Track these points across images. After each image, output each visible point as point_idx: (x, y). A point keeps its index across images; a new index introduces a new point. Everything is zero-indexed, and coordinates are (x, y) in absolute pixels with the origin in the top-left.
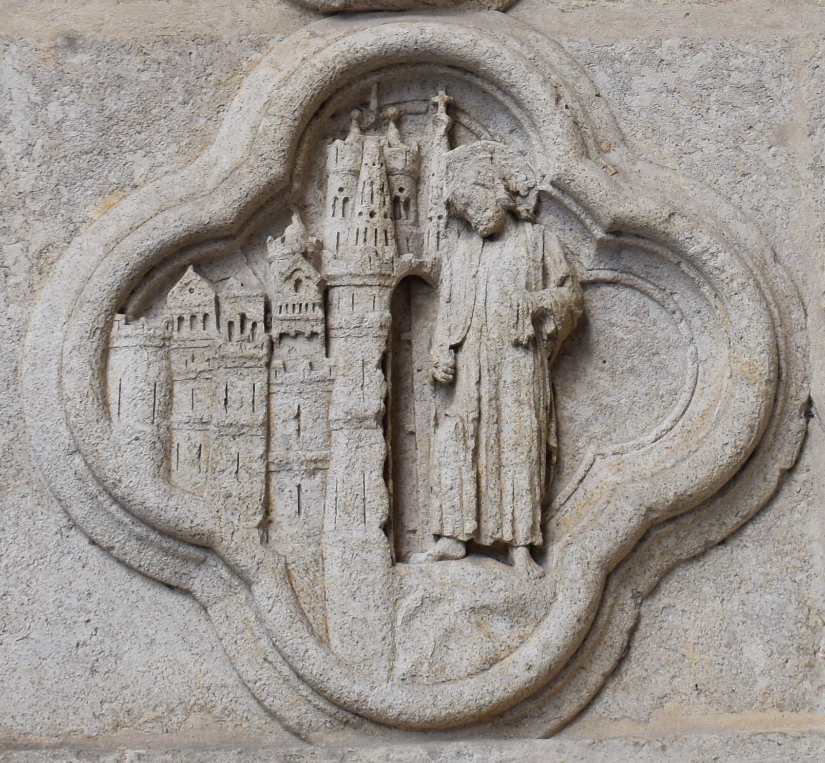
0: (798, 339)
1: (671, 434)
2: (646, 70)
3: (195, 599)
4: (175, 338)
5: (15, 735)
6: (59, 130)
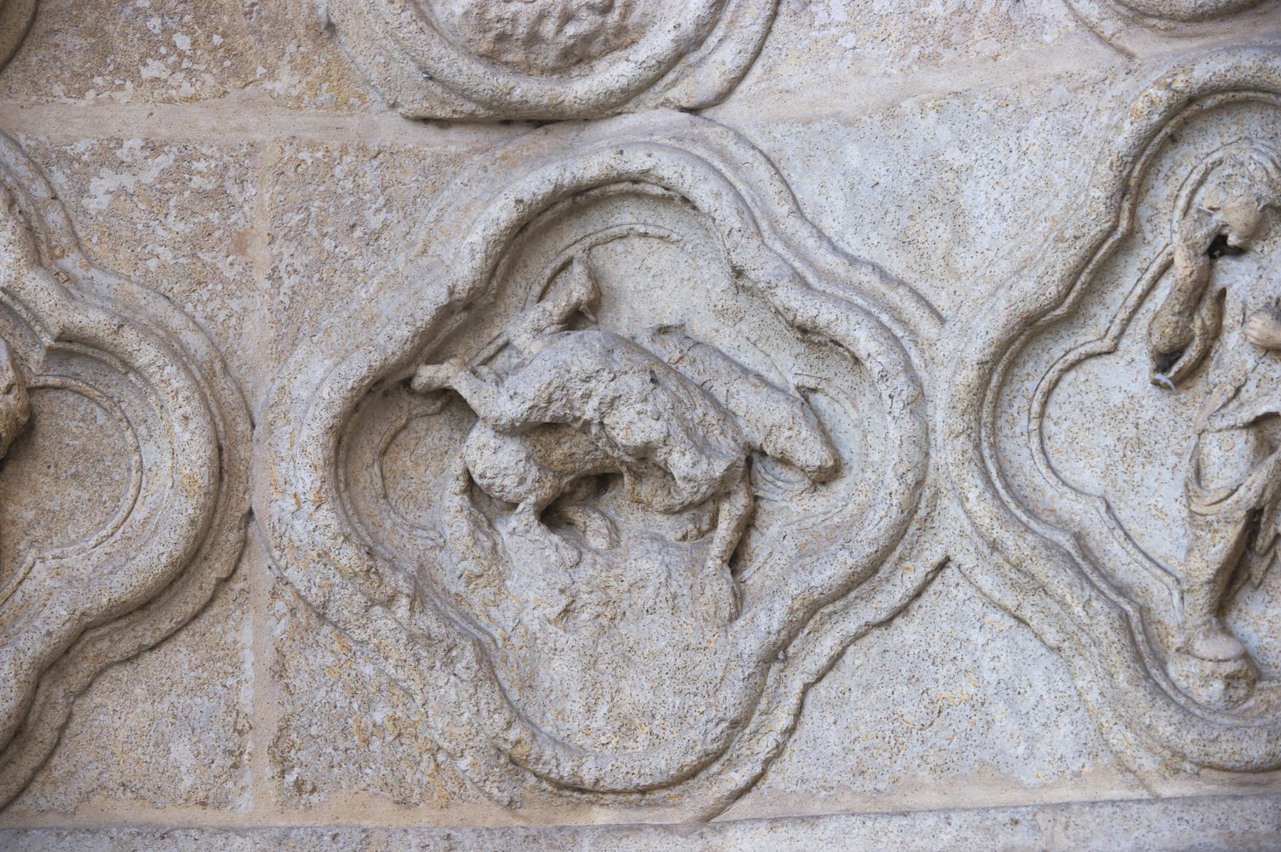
0: (242, 451)
1: (112, 540)
2: (105, 171)
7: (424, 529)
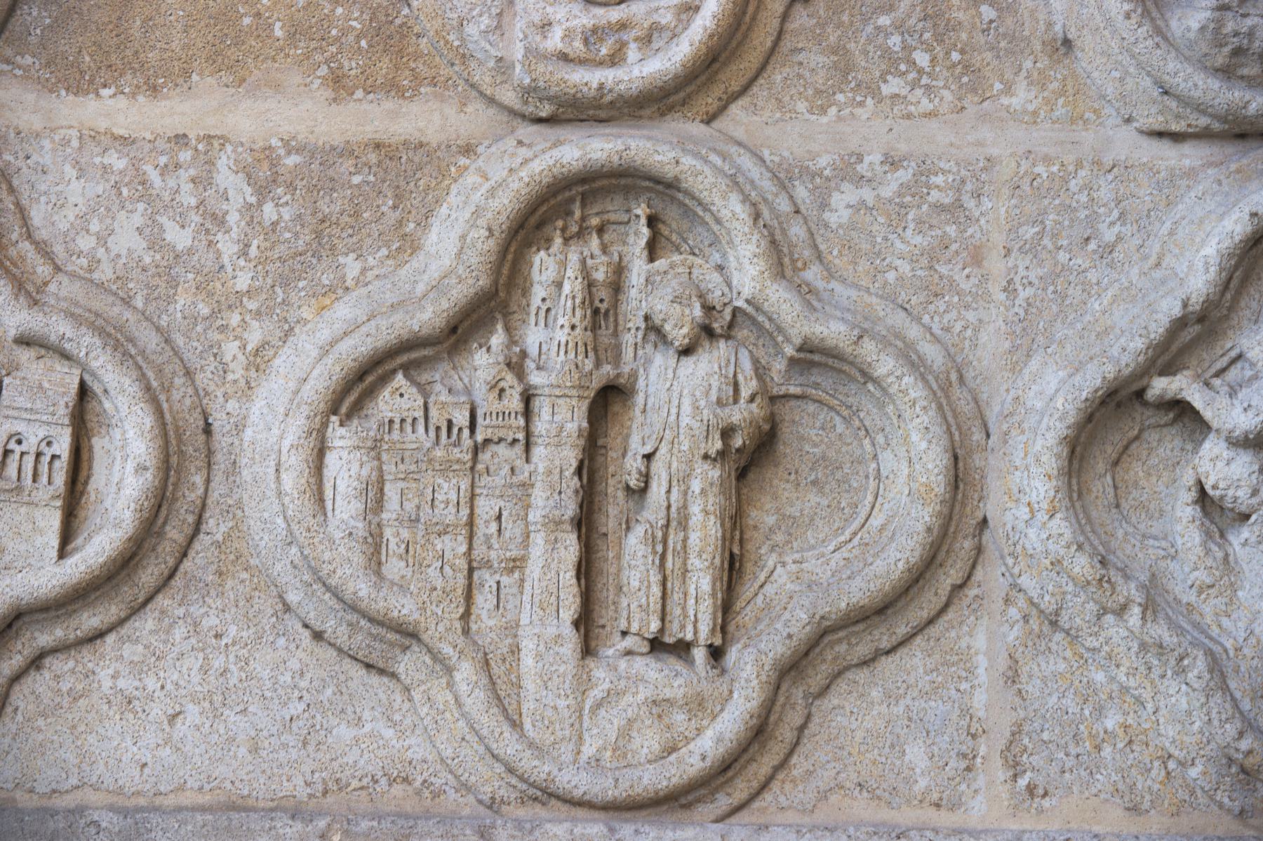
0: (977, 461)
1: (850, 546)
2: (846, 186)
3: (398, 680)
4: (386, 439)
5: (234, 798)
6: (274, 231)
7: (1156, 538)
